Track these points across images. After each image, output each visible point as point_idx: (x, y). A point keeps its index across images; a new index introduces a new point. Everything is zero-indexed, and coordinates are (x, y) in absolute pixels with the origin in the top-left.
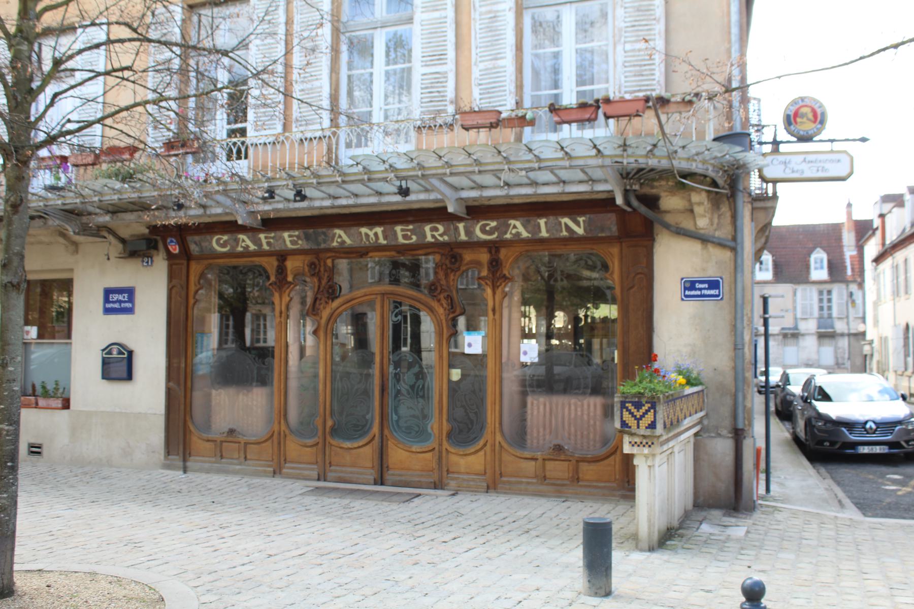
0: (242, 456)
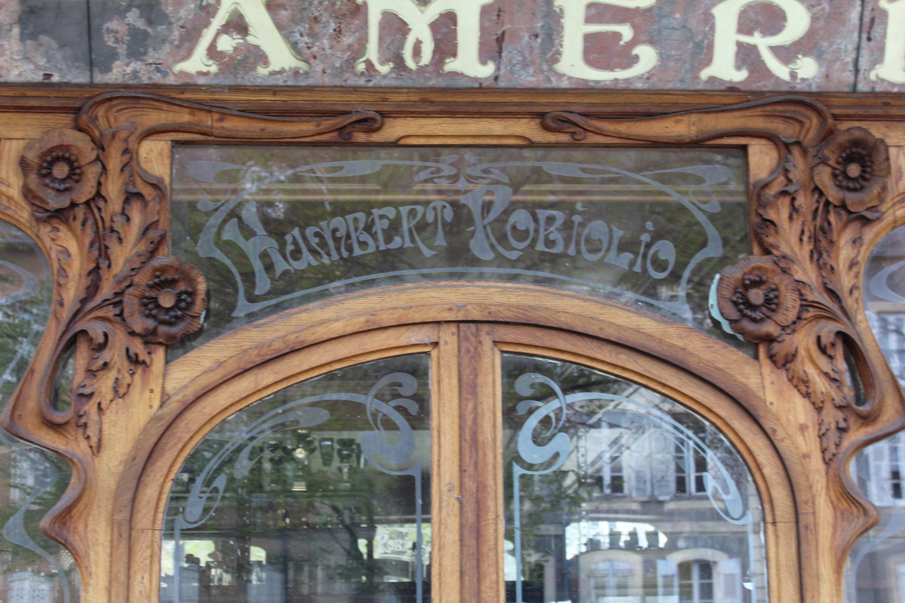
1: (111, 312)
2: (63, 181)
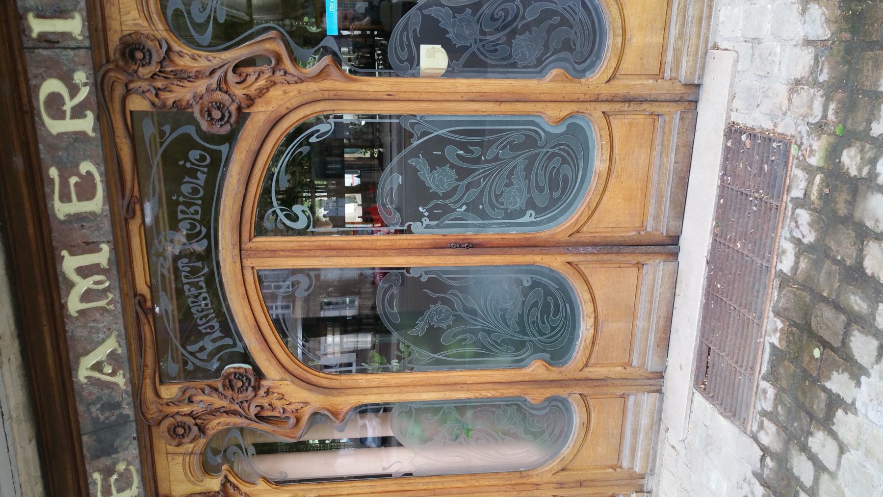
1: (246, 405)
2: (185, 430)
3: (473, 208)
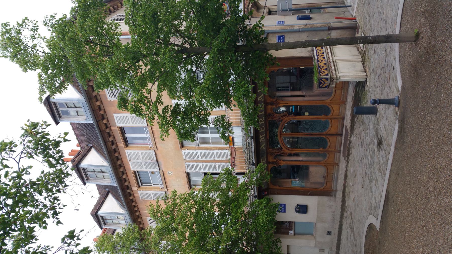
0: (332, 174)
3: (312, 130)
